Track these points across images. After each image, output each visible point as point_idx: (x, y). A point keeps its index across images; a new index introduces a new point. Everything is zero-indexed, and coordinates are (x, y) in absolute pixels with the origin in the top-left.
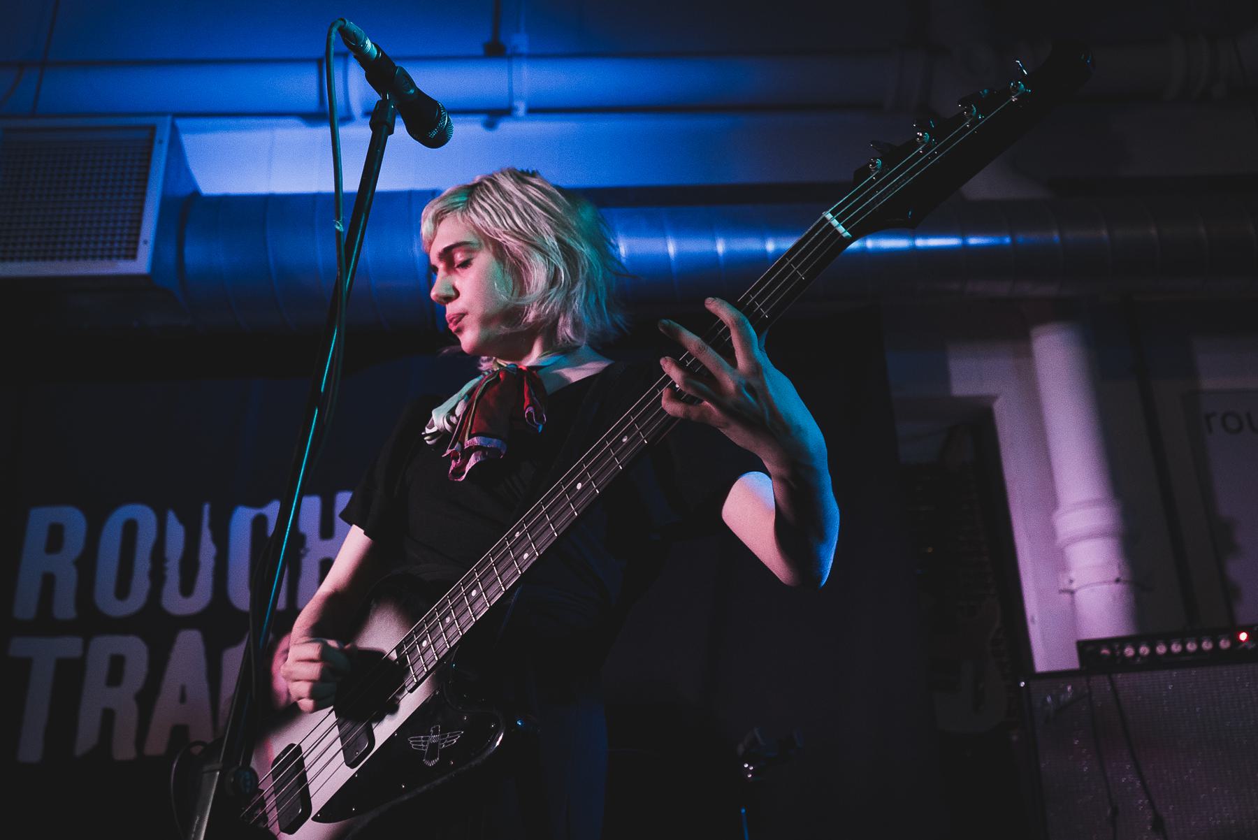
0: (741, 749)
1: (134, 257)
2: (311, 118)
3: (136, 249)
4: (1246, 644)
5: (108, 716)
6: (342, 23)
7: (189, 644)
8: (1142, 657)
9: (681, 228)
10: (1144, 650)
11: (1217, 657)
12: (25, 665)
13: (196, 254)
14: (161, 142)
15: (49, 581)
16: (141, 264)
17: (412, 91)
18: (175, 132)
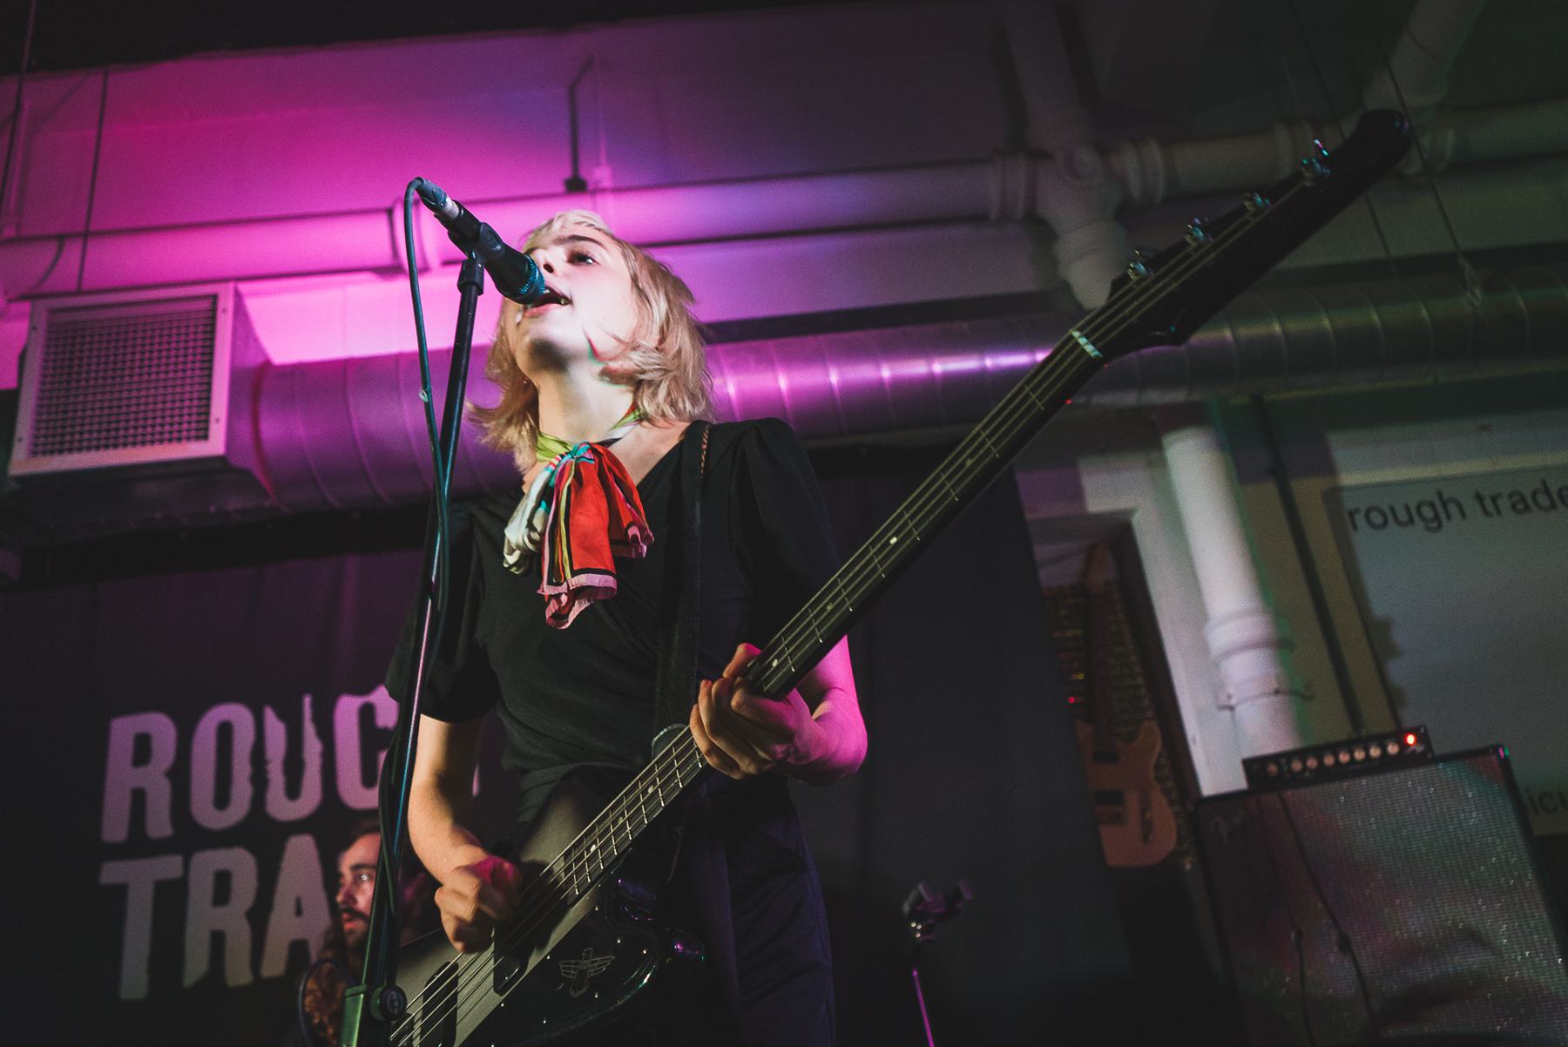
0: (906, 908)
1: (206, 437)
2: (387, 271)
3: (206, 429)
4: (1415, 747)
5: (218, 939)
6: (420, 183)
7: (301, 852)
8: (1311, 771)
9: (791, 360)
10: (1312, 763)
11: (1386, 764)
12: (120, 891)
13: (272, 428)
14: (224, 311)
15: (139, 797)
16: (215, 445)
17: (499, 247)
18: (238, 297)
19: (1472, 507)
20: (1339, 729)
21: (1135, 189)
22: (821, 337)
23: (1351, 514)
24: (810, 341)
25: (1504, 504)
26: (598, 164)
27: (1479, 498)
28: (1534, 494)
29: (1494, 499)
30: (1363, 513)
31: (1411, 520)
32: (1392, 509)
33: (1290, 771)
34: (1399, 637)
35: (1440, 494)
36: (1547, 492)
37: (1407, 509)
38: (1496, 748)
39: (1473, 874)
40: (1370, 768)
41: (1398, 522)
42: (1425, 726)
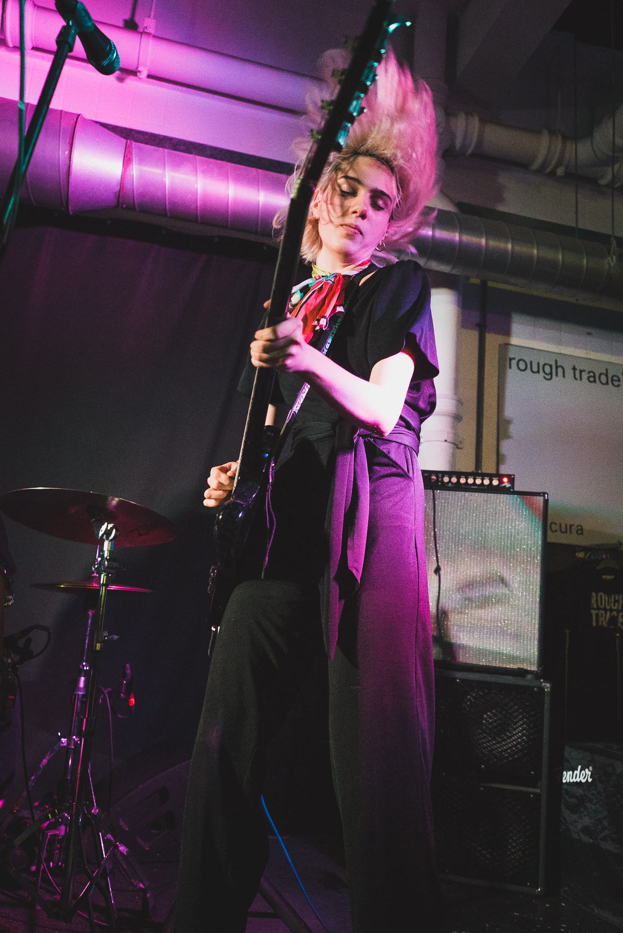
8: (452, 483)
9: (239, 179)
19: (569, 373)
20: (471, 468)
21: (458, 143)
22: (260, 171)
23: (511, 359)
24: (254, 171)
25: (585, 376)
26: (149, 17)
27: (574, 369)
28: (600, 375)
29: (581, 372)
30: (517, 360)
31: (538, 372)
32: (531, 363)
33: (442, 481)
34: (513, 429)
35: (556, 361)
36: (607, 376)
37: (538, 364)
38: (544, 494)
39: (513, 551)
40: (482, 489)
41: (533, 372)
42: (514, 475)
